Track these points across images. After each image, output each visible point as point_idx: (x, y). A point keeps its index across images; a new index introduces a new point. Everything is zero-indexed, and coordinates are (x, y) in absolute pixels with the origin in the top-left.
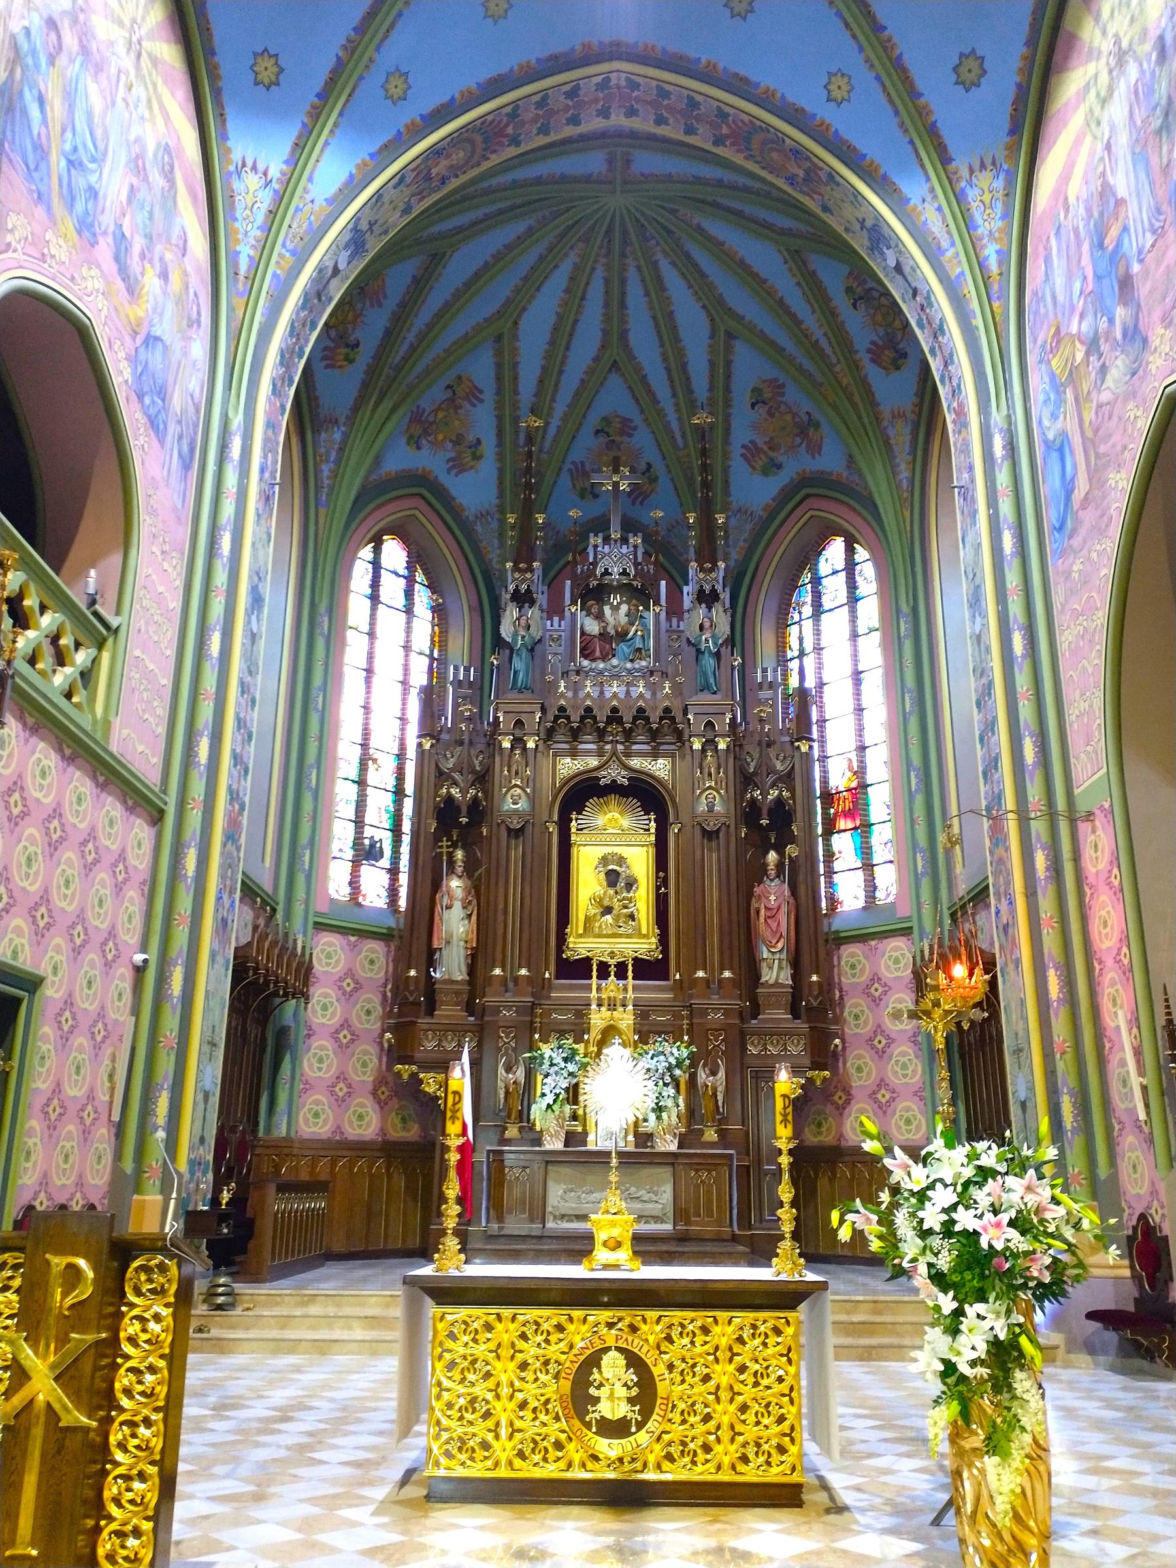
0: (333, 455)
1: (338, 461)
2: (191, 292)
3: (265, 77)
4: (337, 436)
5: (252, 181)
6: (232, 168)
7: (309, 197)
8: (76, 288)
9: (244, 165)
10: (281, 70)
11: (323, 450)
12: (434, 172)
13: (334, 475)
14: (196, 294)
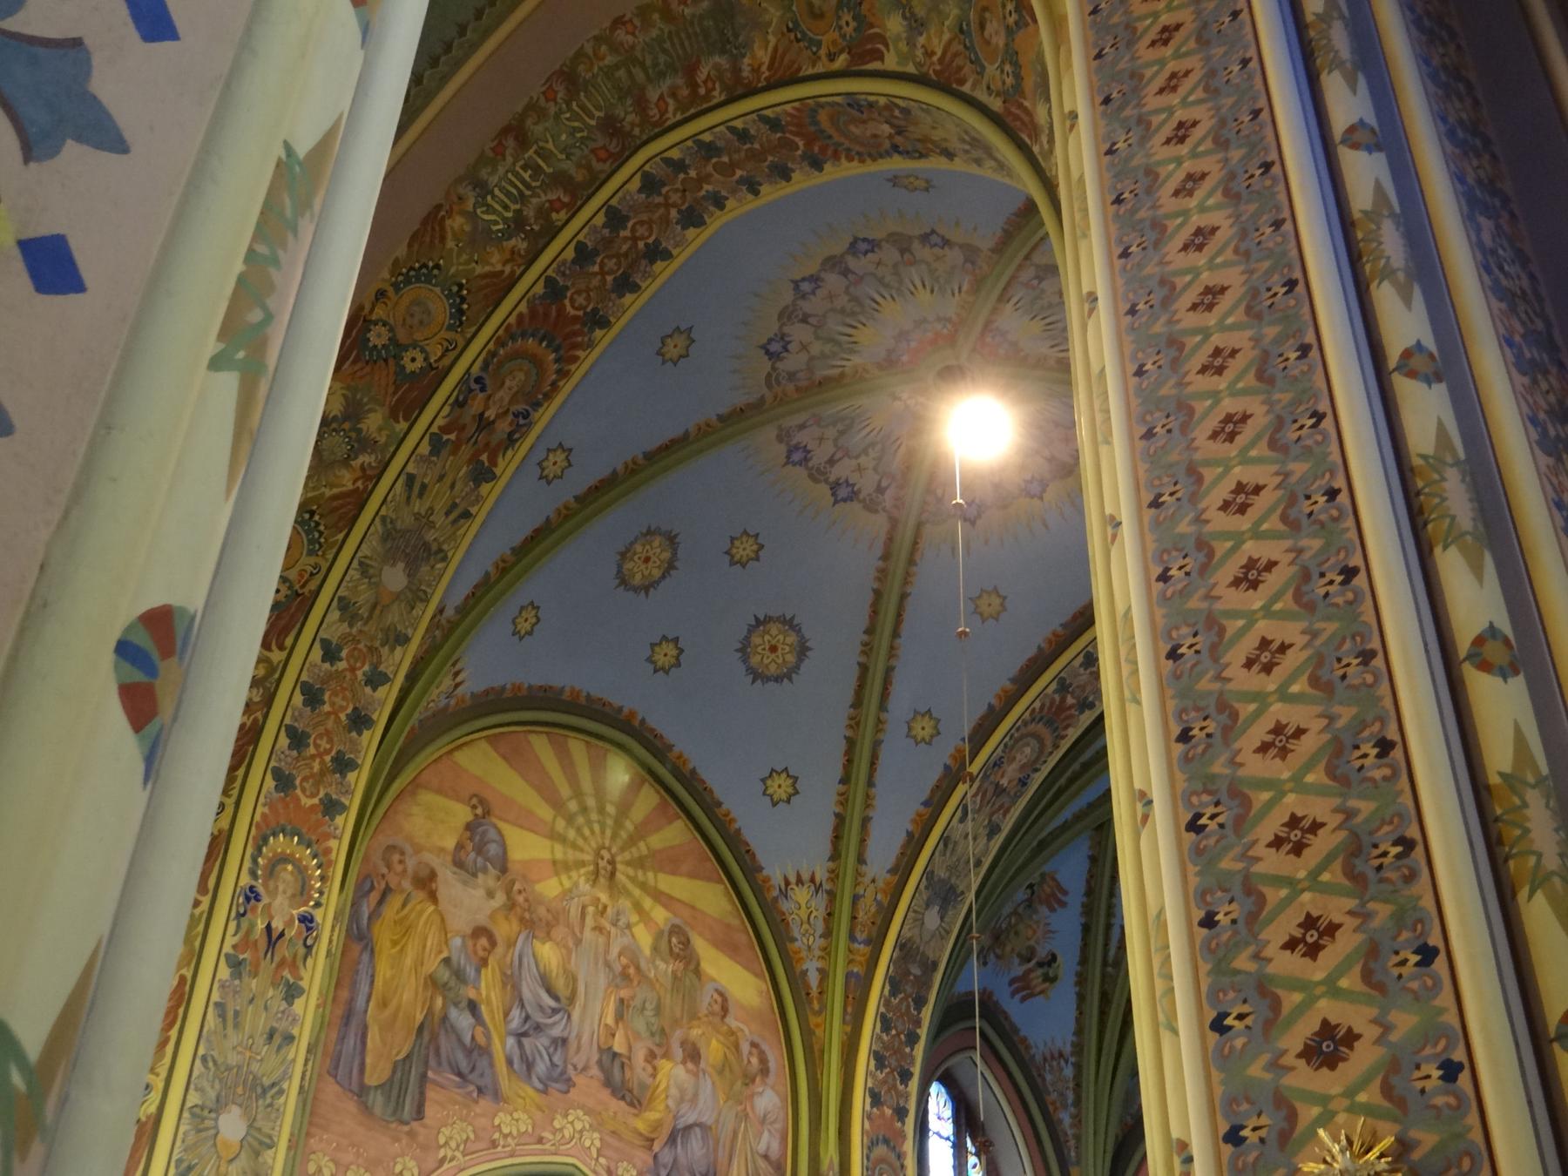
0: (1071, 1097)
1: (1078, 1102)
4: (1069, 1072)
5: (801, 895)
6: (775, 893)
7: (867, 880)
8: (547, 1146)
9: (787, 883)
10: (796, 779)
11: (1054, 1096)
12: (1004, 782)
13: (1078, 1120)
14: (754, 1045)
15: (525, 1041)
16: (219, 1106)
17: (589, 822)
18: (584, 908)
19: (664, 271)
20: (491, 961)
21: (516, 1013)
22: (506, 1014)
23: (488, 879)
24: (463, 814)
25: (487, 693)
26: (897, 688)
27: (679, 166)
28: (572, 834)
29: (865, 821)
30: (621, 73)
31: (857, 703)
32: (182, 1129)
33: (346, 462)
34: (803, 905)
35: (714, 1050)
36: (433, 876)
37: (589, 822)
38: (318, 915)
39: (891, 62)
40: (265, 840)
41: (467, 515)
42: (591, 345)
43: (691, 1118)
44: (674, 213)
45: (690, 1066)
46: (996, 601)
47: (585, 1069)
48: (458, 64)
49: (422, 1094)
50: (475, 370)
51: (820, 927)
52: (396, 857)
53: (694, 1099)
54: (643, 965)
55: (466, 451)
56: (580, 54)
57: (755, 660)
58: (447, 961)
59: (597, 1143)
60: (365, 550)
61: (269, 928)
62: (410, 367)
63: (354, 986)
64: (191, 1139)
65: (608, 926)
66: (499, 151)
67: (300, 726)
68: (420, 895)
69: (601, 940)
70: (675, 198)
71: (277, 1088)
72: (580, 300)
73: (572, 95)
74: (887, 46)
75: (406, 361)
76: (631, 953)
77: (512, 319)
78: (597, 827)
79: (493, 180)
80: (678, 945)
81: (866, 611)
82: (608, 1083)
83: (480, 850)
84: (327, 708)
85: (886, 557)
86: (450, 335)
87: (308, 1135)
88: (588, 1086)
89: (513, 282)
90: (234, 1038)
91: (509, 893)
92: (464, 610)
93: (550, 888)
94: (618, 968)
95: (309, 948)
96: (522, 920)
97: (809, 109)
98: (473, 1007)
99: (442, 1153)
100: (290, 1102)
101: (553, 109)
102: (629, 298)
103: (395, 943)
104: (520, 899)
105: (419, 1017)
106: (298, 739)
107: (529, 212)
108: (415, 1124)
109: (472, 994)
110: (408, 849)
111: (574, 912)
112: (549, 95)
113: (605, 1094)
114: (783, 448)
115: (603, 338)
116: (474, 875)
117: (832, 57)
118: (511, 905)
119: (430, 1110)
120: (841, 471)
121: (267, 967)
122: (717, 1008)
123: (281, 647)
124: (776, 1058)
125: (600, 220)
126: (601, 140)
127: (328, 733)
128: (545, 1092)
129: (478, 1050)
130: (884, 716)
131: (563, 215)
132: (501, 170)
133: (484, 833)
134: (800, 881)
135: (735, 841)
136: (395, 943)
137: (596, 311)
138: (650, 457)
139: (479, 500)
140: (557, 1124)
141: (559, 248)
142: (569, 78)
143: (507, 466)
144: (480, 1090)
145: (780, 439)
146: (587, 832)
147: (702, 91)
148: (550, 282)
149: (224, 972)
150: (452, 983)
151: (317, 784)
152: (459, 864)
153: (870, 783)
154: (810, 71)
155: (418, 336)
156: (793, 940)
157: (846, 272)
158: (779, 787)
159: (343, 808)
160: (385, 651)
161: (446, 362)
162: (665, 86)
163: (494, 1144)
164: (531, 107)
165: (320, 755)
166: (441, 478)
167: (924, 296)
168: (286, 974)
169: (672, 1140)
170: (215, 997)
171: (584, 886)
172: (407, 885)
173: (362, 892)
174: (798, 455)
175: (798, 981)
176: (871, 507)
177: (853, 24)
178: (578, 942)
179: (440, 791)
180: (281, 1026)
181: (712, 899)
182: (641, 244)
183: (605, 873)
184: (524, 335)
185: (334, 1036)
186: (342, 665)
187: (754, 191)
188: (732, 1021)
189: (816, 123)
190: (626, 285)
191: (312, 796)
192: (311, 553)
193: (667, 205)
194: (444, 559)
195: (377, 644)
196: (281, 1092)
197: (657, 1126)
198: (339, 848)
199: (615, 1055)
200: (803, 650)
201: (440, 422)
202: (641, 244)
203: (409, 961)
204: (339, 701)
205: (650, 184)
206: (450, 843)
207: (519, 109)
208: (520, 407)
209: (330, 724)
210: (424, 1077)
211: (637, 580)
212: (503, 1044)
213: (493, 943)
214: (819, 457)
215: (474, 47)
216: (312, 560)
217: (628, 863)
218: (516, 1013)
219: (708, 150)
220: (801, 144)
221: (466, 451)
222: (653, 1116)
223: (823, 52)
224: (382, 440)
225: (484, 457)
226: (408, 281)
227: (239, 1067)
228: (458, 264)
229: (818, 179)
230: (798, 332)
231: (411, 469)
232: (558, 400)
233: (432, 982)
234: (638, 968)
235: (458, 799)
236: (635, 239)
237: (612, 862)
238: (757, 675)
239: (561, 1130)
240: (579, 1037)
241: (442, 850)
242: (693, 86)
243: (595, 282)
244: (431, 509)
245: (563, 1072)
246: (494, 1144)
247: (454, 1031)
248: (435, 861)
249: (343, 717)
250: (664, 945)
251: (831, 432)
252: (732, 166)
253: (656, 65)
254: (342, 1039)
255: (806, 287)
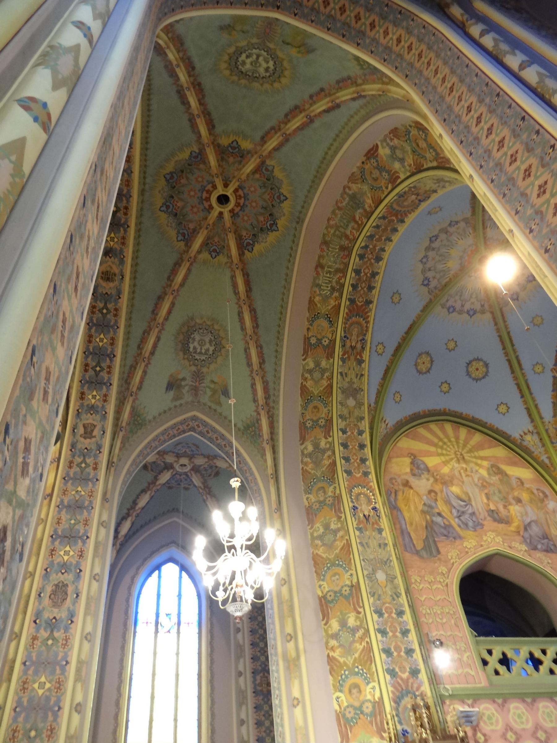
2: (535, 492)
3: (504, 411)
5: (528, 438)
6: (519, 441)
7: (547, 423)
8: (485, 547)
9: (522, 436)
10: (506, 404)
14: (538, 490)
15: (461, 518)
16: (374, 572)
17: (448, 446)
18: (459, 472)
19: (379, 278)
20: (438, 499)
21: (454, 511)
22: (451, 512)
23: (425, 475)
24: (408, 460)
25: (397, 423)
26: (523, 362)
27: (366, 247)
28: (444, 452)
29: (536, 406)
30: (337, 232)
31: (513, 372)
32: (366, 582)
33: (322, 378)
34: (530, 441)
35: (525, 496)
36: (407, 482)
37: (448, 446)
38: (377, 506)
39: (402, 177)
40: (352, 491)
41: (362, 375)
42: (371, 310)
43: (529, 520)
44: (372, 261)
45: (519, 504)
46: (539, 319)
47: (485, 518)
48: (295, 258)
49: (436, 546)
50: (343, 335)
51: (540, 445)
52: (394, 481)
53: (527, 513)
54: (488, 480)
55: (352, 358)
56: (324, 235)
57: (473, 376)
58: (425, 504)
59: (501, 539)
60: (339, 399)
61: (364, 515)
62: (325, 344)
63: (400, 523)
64: (371, 584)
65: (470, 474)
66: (318, 273)
67: (346, 455)
68: (406, 489)
69: (470, 479)
70: (370, 256)
71: (389, 560)
72: (361, 299)
73: (328, 247)
74: (398, 173)
75: (324, 343)
76: (482, 478)
77: (345, 315)
78: (451, 447)
79: (320, 282)
80: (495, 470)
81: (500, 344)
82: (495, 520)
83: (418, 468)
84: (351, 447)
85: (496, 324)
86: (331, 329)
87: (407, 571)
88: (489, 523)
89: (340, 305)
90: (369, 551)
91: (433, 476)
92: (376, 402)
93: (446, 470)
94: (480, 485)
95: (379, 517)
96: (442, 483)
97: (390, 207)
98: (439, 514)
99: (452, 561)
100: (395, 563)
101: (325, 253)
102: (374, 291)
103: (406, 505)
104: (438, 477)
105: (424, 524)
106: (347, 459)
107: (334, 284)
108: (439, 556)
109: (437, 511)
110: (396, 477)
111: (457, 474)
112: (322, 250)
113: (496, 524)
114: (445, 310)
115: (373, 306)
116: (420, 476)
117: (387, 188)
118: (436, 480)
119: (441, 550)
120: (467, 307)
121: (369, 526)
122: (519, 483)
123: (330, 437)
124: (548, 491)
125: (353, 275)
126: (342, 254)
127: (354, 454)
128: (475, 531)
129: (448, 527)
130: (523, 371)
131: (343, 280)
132: (321, 278)
133: (417, 463)
134: (525, 434)
135: (497, 431)
136: (406, 505)
137: (366, 300)
138: (407, 333)
139: (363, 369)
140: (485, 538)
141: (347, 288)
142: (325, 243)
143: (366, 356)
144: (455, 538)
145: (443, 308)
146: (449, 449)
147: (360, 222)
148: (350, 300)
149: (357, 533)
150: (429, 510)
151: (359, 470)
152: (414, 475)
153: (531, 394)
154: (384, 196)
155: (323, 334)
156: (533, 452)
157: (433, 249)
158: (503, 409)
159: (370, 473)
160: (359, 424)
161: (334, 337)
162: (350, 228)
163: (467, 553)
164: (320, 257)
165: (355, 461)
166: (349, 369)
167: (461, 242)
168: (376, 526)
169: (526, 529)
170: (358, 541)
171: (456, 465)
172: (401, 487)
173: (388, 495)
174: (451, 310)
175: (542, 464)
176: (483, 312)
177: (387, 174)
178: (463, 482)
179: (398, 457)
180: (381, 542)
181: (500, 452)
182: (369, 275)
183: (461, 459)
184: (350, 318)
185: (401, 539)
186: (349, 433)
187: (391, 240)
188: (527, 485)
189: (394, 209)
190: (371, 288)
191: (359, 473)
192: (325, 407)
193: (369, 260)
194: (362, 390)
195: (356, 423)
196: (391, 561)
197: (518, 527)
198: (374, 485)
199: (493, 511)
200: (486, 365)
201: (341, 354)
202: (369, 275)
203: (413, 508)
204: (353, 444)
205: (361, 257)
206: (408, 470)
207: (317, 259)
208: (361, 338)
209: (354, 451)
210: (435, 542)
211: (424, 370)
212: (455, 521)
213: (436, 493)
214: (458, 306)
215: (296, 251)
216: (327, 409)
217: (468, 452)
218: (454, 511)
219: (371, 237)
220: (394, 218)
221: (352, 358)
222: (515, 524)
223: (384, 188)
224: (328, 367)
225: (358, 357)
226: (313, 321)
227: (375, 558)
228: (323, 310)
229: (406, 225)
230: (430, 275)
231: (340, 371)
232: (370, 330)
233: (423, 512)
234: (487, 482)
235: (404, 456)
236: (366, 274)
237: (461, 454)
238: (477, 380)
239: (487, 540)
240: (478, 510)
241: (407, 473)
242: (356, 222)
243: (362, 292)
244: (351, 379)
245: (479, 522)
246: (467, 553)
247: (437, 523)
248: (406, 477)
249: (356, 447)
250: (491, 472)
251: (457, 298)
252: (380, 237)
253: (344, 224)
254: (404, 539)
255: (424, 260)
